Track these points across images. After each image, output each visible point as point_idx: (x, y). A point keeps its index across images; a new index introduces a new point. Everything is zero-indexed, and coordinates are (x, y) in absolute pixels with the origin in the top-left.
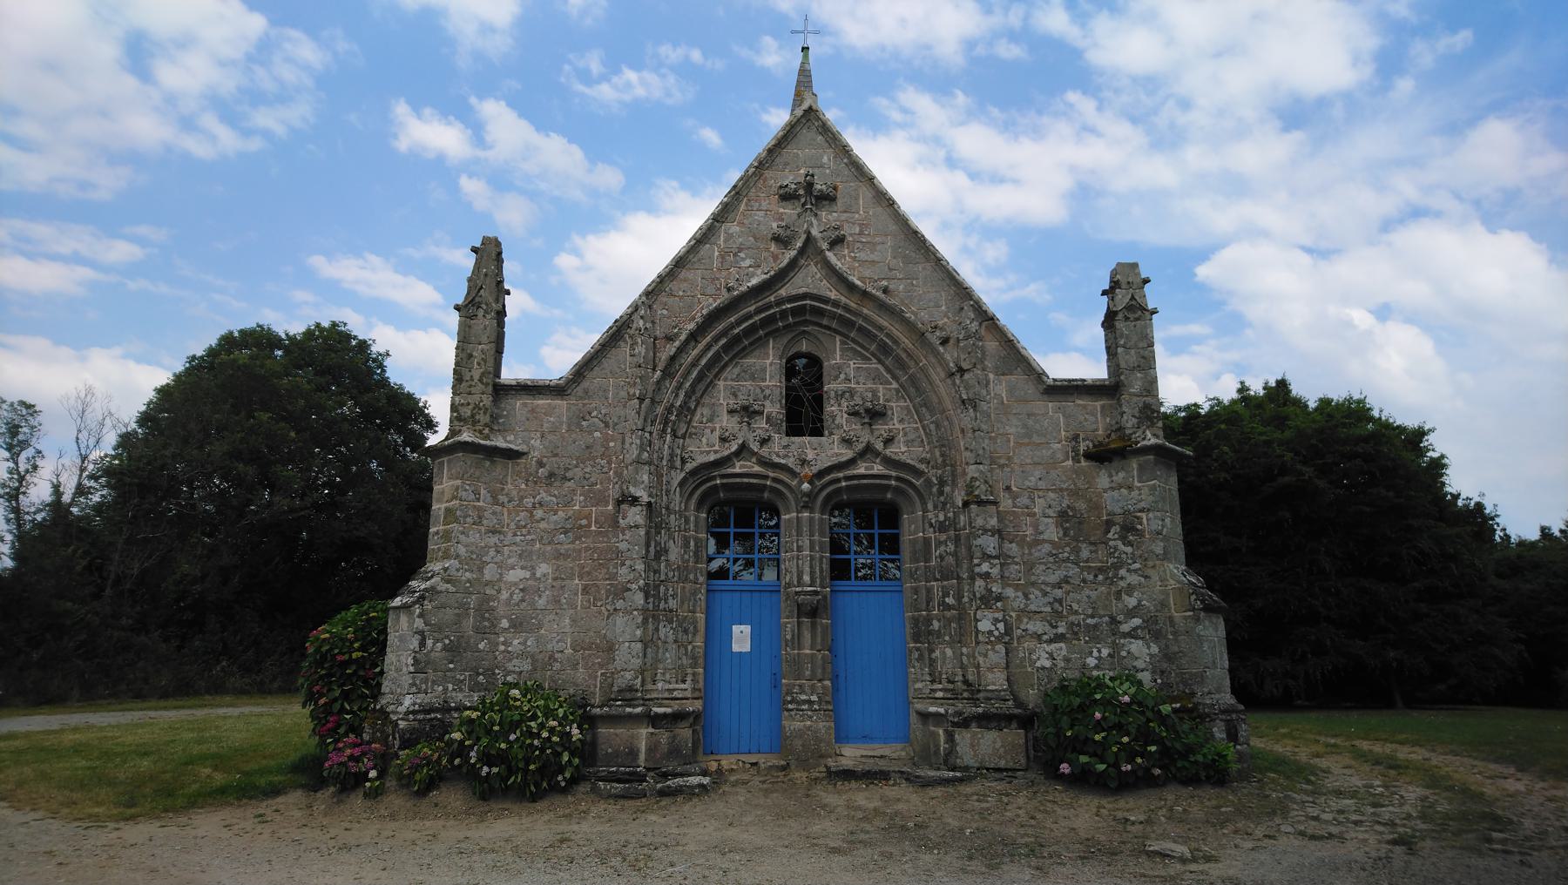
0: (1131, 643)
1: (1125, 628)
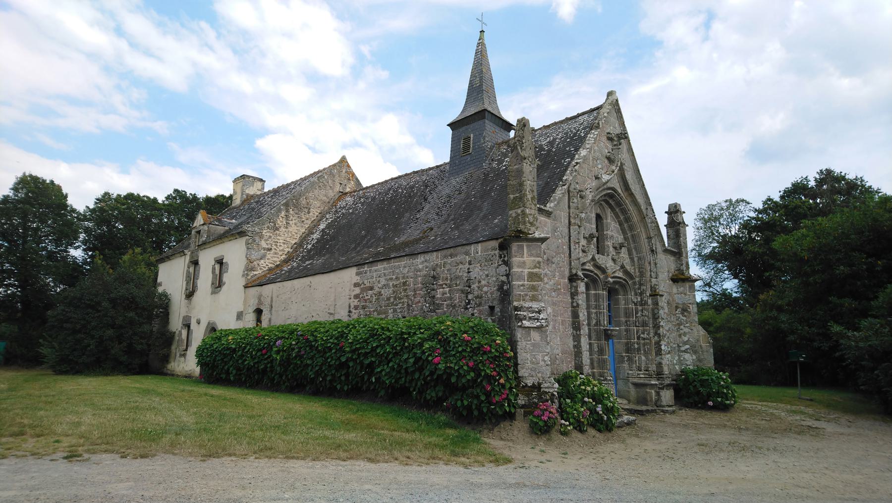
1: (683, 349)
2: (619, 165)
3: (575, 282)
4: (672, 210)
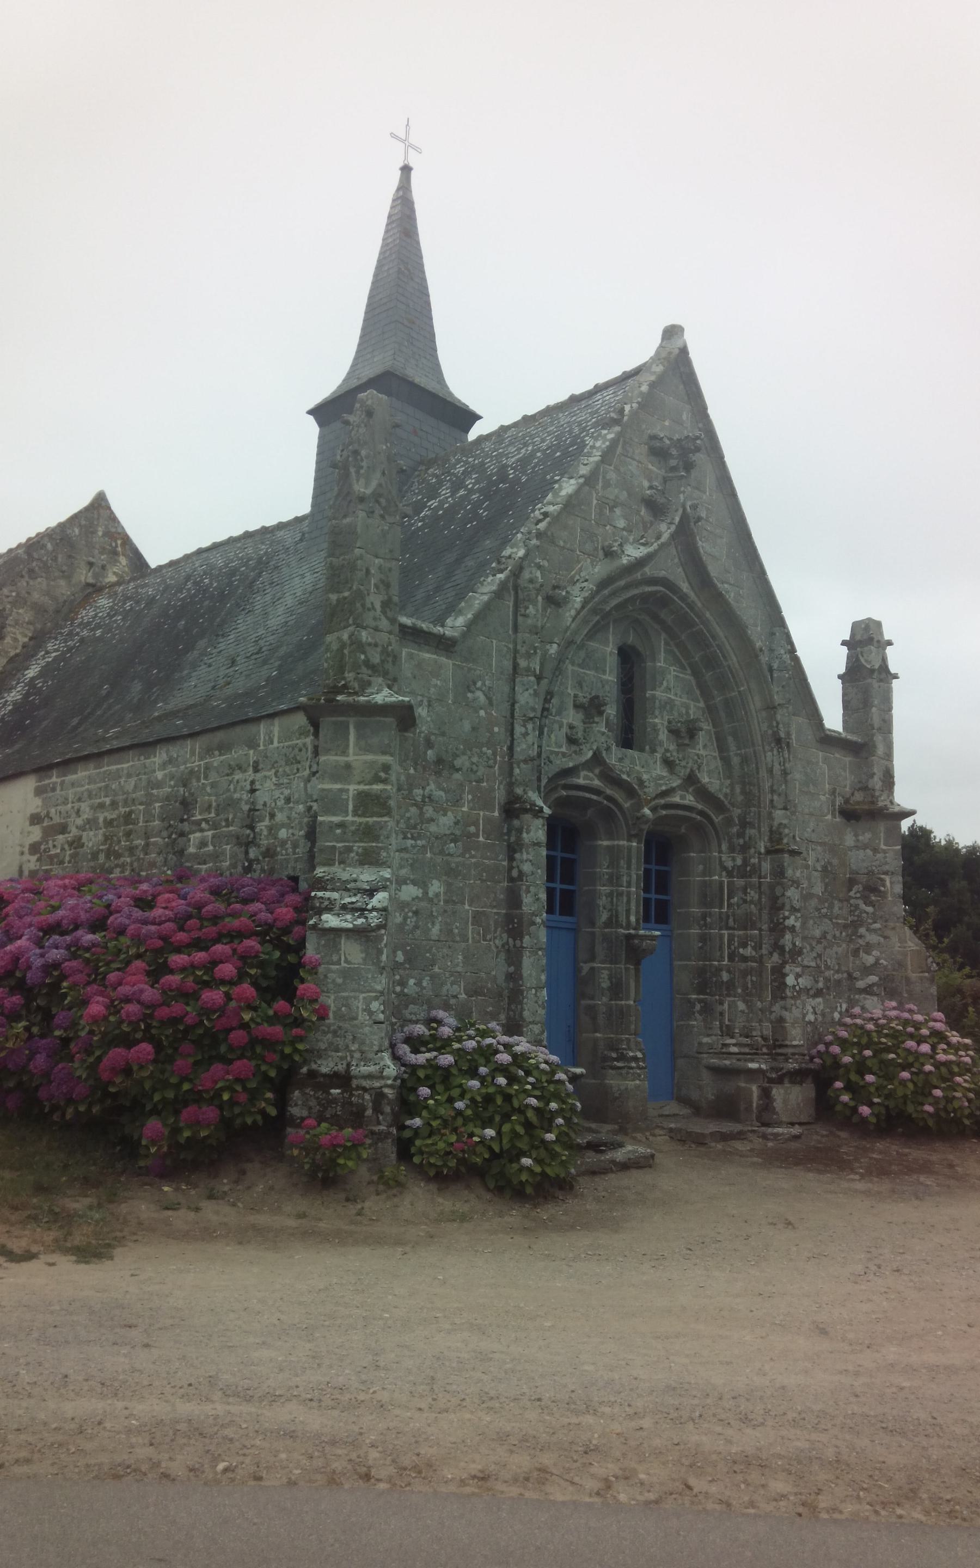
0: (865, 999)
1: (861, 984)
2: (677, 519)
3: (517, 817)
4: (858, 637)
